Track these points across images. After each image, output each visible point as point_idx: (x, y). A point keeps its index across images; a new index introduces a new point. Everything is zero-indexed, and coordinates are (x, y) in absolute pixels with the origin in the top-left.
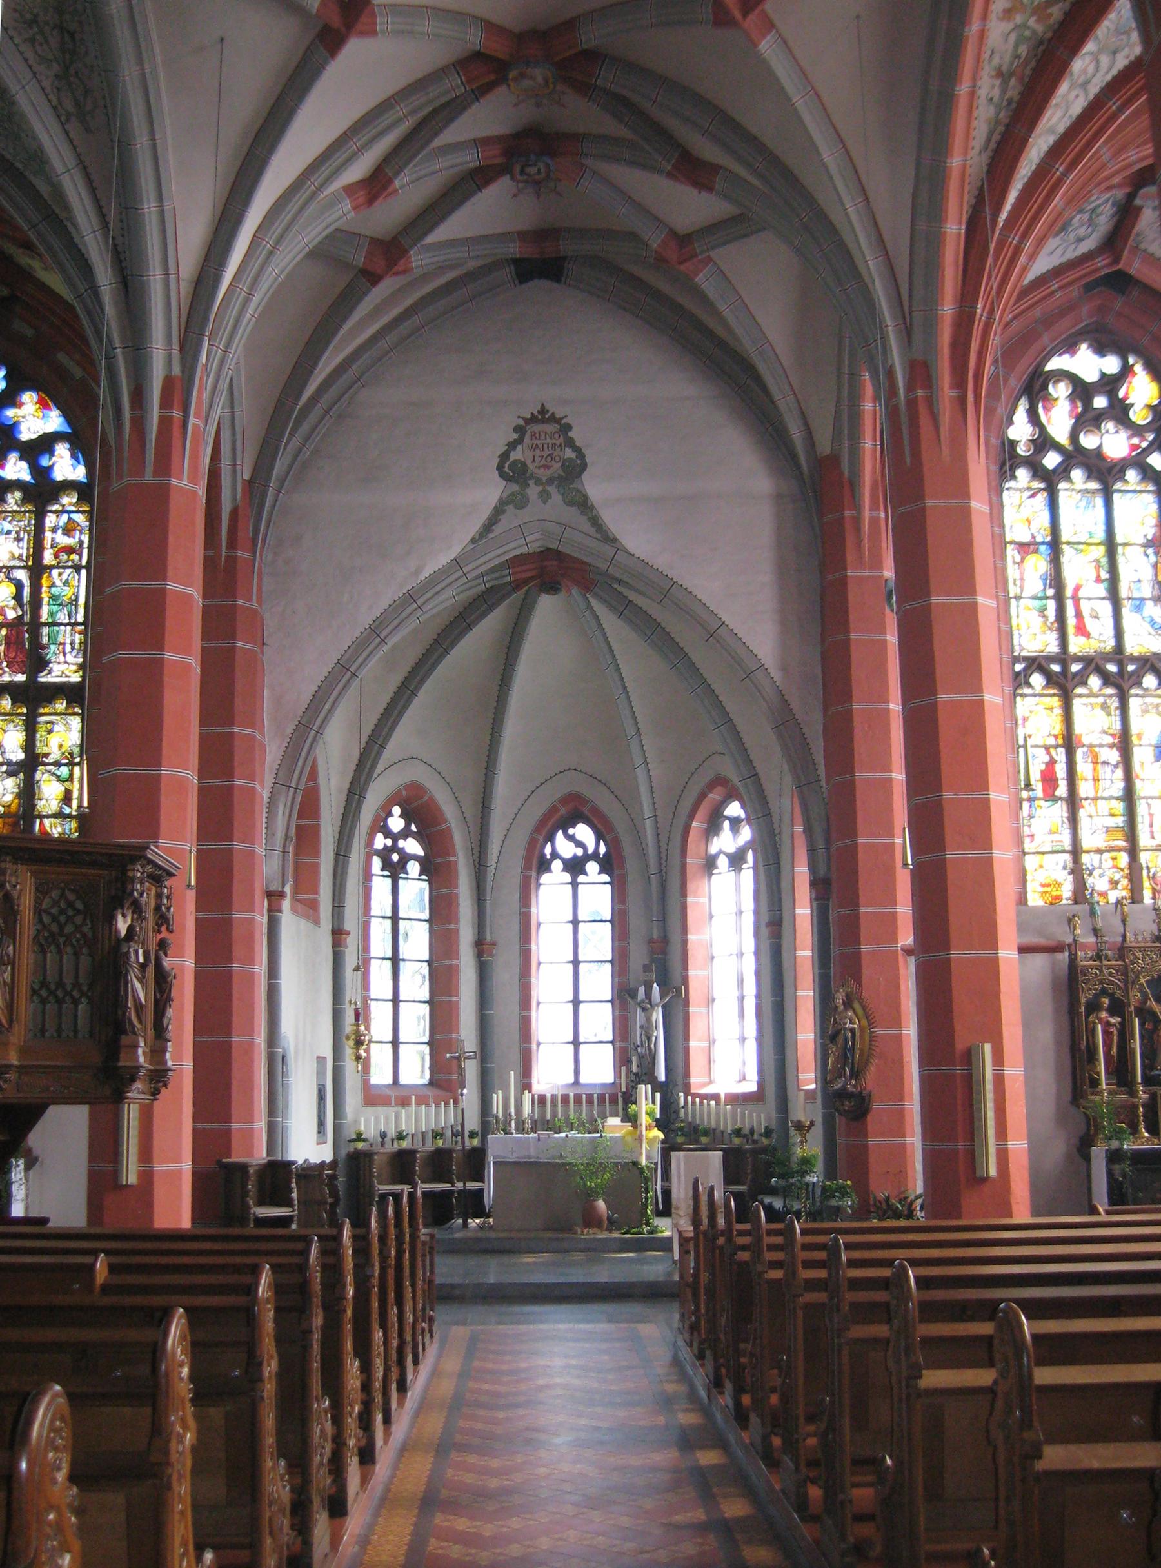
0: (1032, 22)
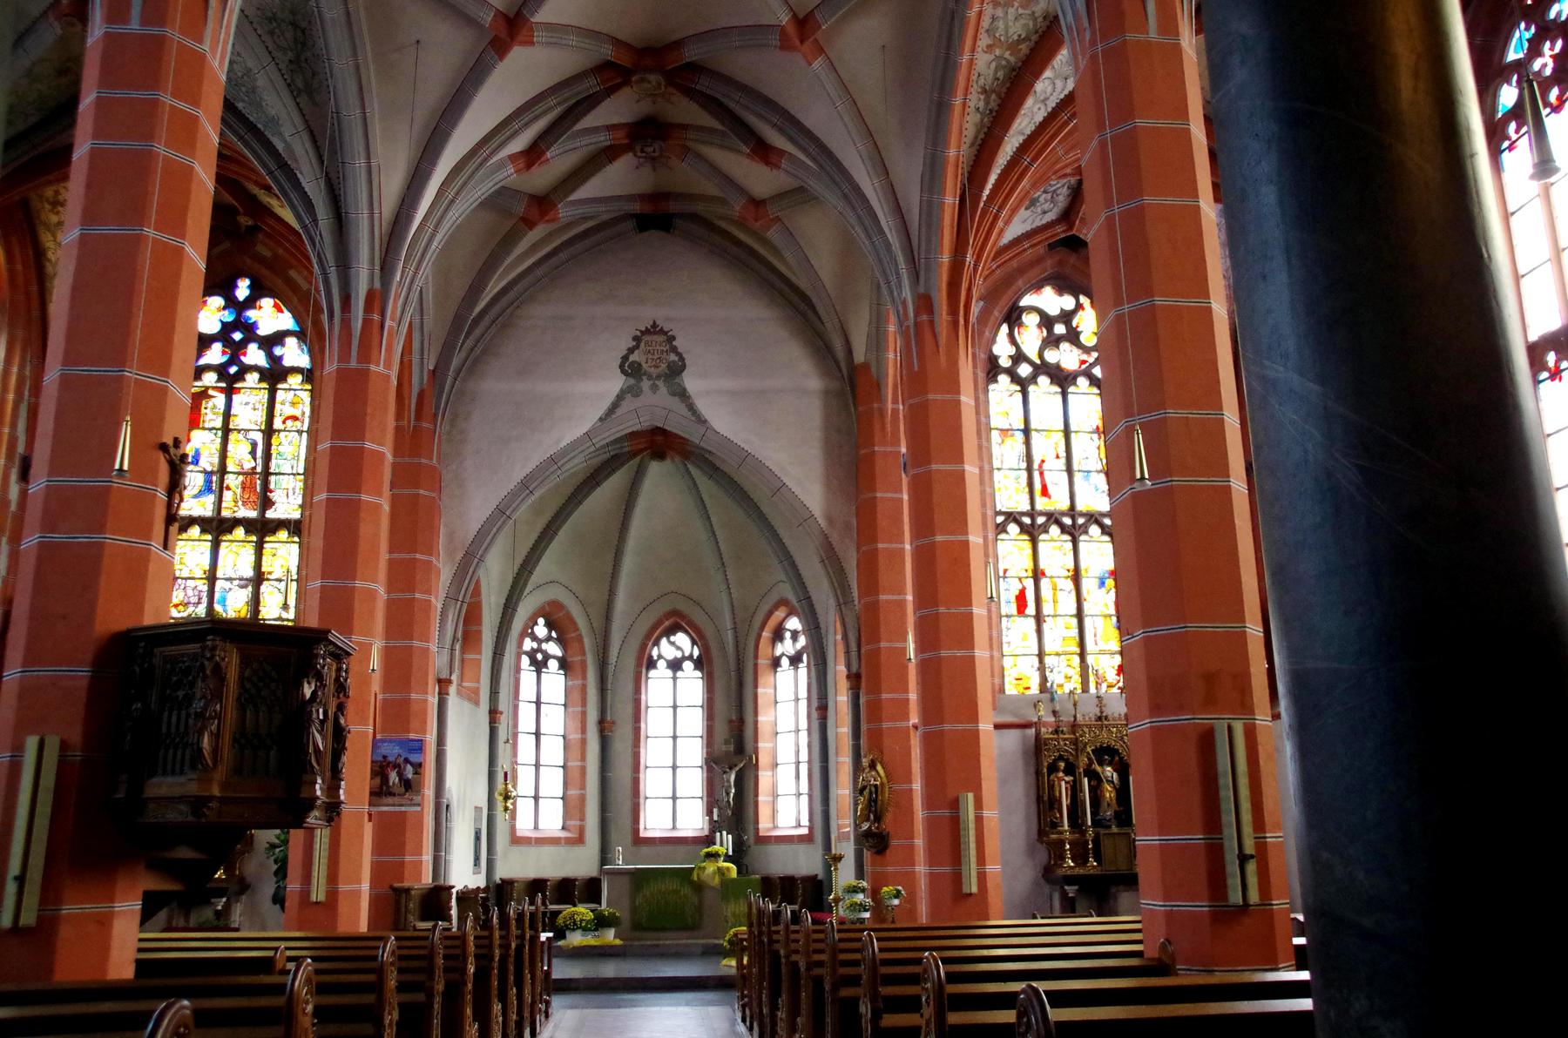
0: (1007, 55)
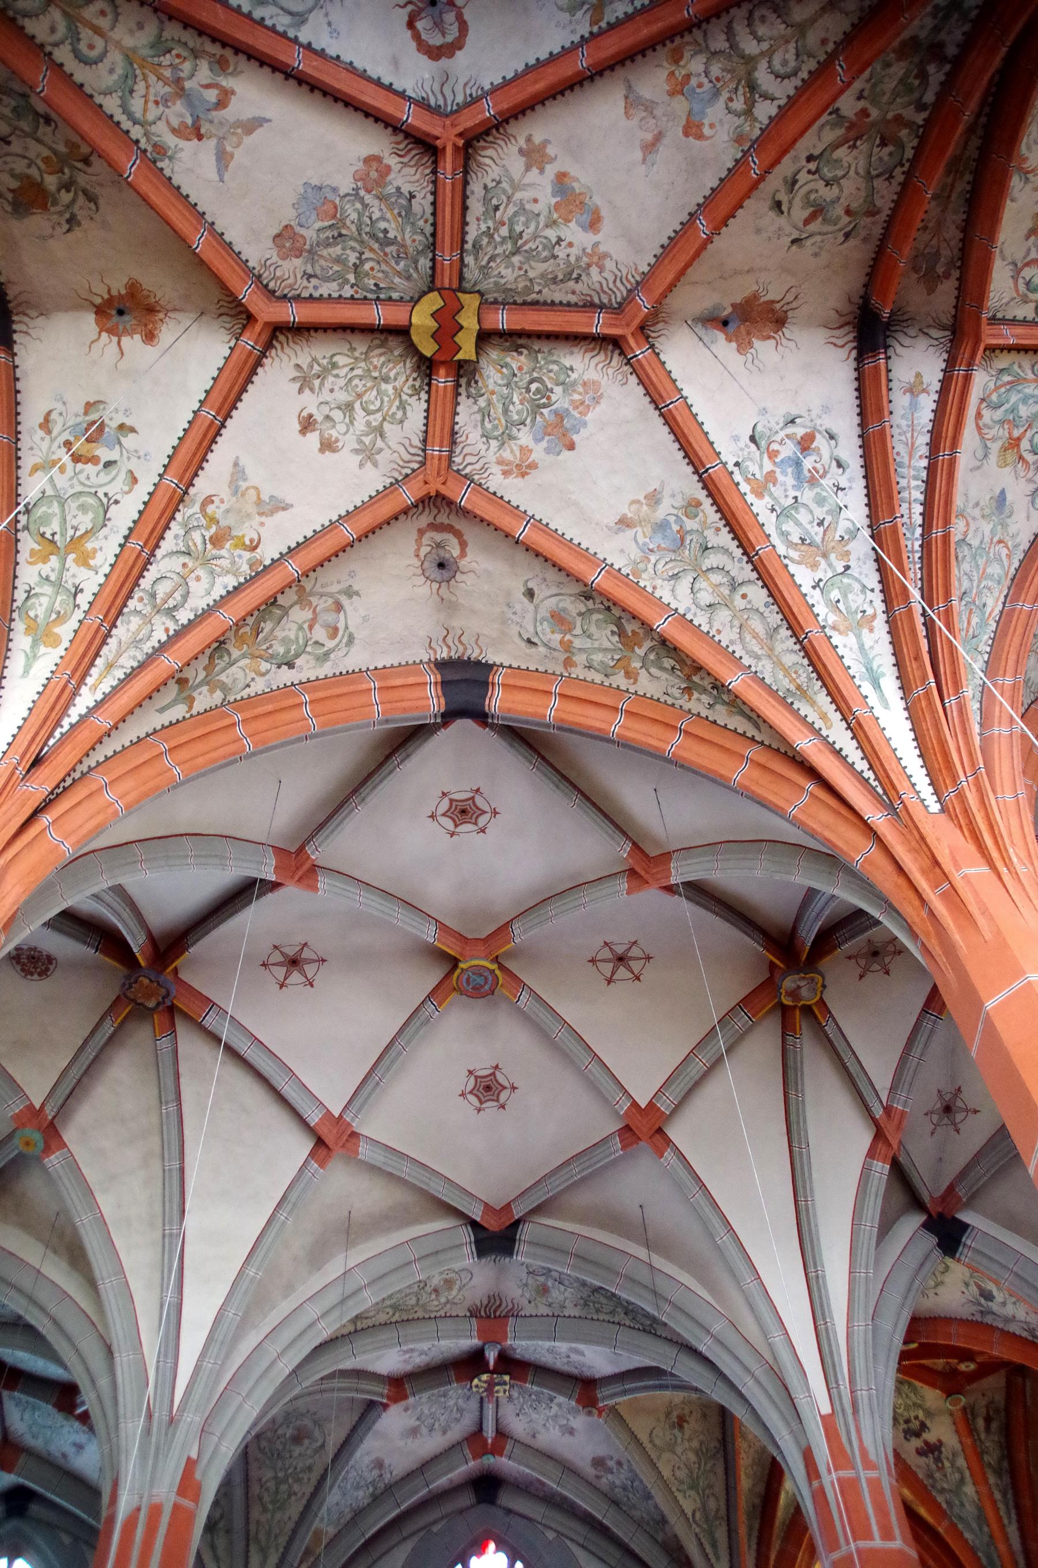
0: (640, 652)
